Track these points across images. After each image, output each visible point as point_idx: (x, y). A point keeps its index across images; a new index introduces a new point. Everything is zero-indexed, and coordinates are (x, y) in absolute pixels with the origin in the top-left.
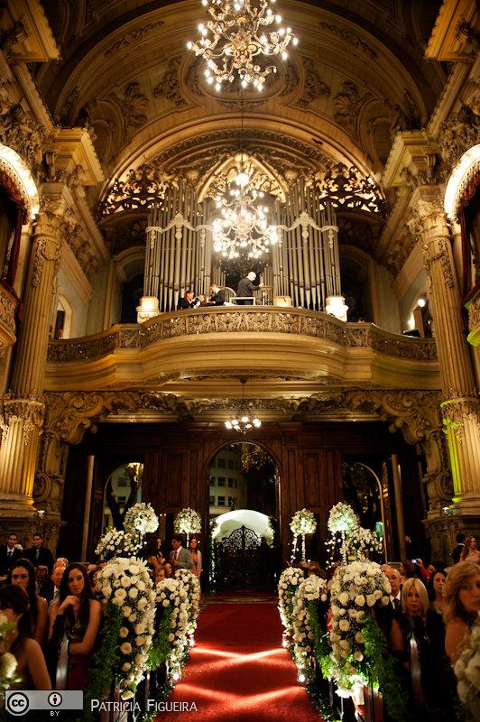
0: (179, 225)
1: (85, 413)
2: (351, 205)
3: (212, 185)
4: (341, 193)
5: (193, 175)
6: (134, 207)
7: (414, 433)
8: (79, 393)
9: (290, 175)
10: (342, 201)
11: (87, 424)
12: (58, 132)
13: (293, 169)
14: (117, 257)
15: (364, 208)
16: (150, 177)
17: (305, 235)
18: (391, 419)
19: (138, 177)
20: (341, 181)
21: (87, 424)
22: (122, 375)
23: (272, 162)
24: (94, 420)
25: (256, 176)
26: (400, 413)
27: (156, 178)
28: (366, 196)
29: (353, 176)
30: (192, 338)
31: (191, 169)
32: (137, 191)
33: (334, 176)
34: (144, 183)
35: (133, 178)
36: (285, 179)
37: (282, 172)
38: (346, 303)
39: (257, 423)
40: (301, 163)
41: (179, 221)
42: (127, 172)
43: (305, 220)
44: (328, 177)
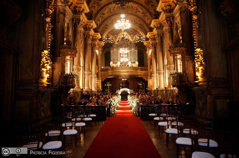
0: (115, 50)
1: (105, 78)
2: (141, 41)
3: (119, 38)
4: (140, 39)
5: (116, 35)
6: (107, 42)
7: (146, 80)
8: (104, 75)
9: (132, 35)
10: (140, 41)
11: (105, 79)
12: (99, 42)
13: (132, 34)
14: (104, 50)
15: (144, 42)
16: (109, 37)
17: (133, 52)
18: (143, 78)
19: (107, 37)
20: (140, 37)
21: (105, 79)
22: (110, 74)
23: (129, 32)
24: (106, 79)
25: (126, 36)
26: (145, 78)
27: (110, 37)
28: (144, 40)
29: (142, 36)
30: (118, 70)
31: (115, 34)
32: (107, 39)
33: (139, 36)
34: (108, 38)
35: (106, 37)
36: (131, 36)
37: (130, 35)
38: (138, 62)
39: (126, 79)
40: (134, 33)
41: (115, 50)
42: (105, 36)
43: (133, 49)
44: (138, 36)
